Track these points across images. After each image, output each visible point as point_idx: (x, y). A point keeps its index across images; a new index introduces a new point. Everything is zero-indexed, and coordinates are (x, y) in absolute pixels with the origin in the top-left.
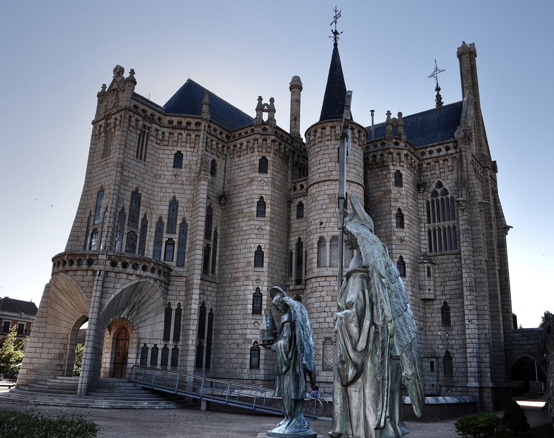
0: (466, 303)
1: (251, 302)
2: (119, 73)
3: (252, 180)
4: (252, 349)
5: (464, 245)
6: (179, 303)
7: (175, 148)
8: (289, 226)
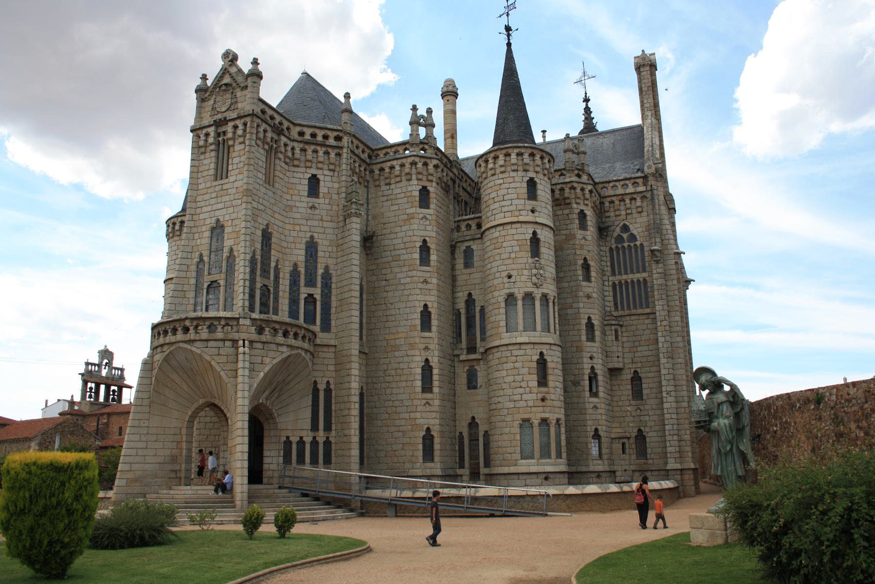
0: (663, 372)
1: (419, 377)
3: (411, 217)
4: (424, 438)
5: (660, 303)
6: (328, 382)
7: (309, 170)
8: (454, 279)
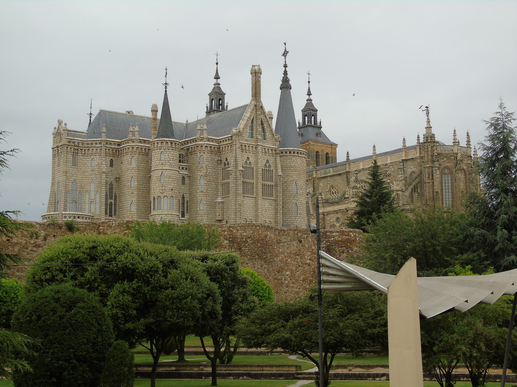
2: (60, 123)
